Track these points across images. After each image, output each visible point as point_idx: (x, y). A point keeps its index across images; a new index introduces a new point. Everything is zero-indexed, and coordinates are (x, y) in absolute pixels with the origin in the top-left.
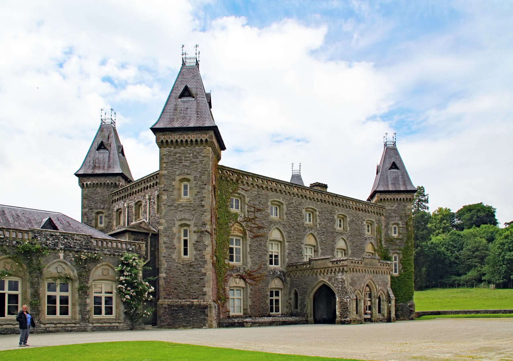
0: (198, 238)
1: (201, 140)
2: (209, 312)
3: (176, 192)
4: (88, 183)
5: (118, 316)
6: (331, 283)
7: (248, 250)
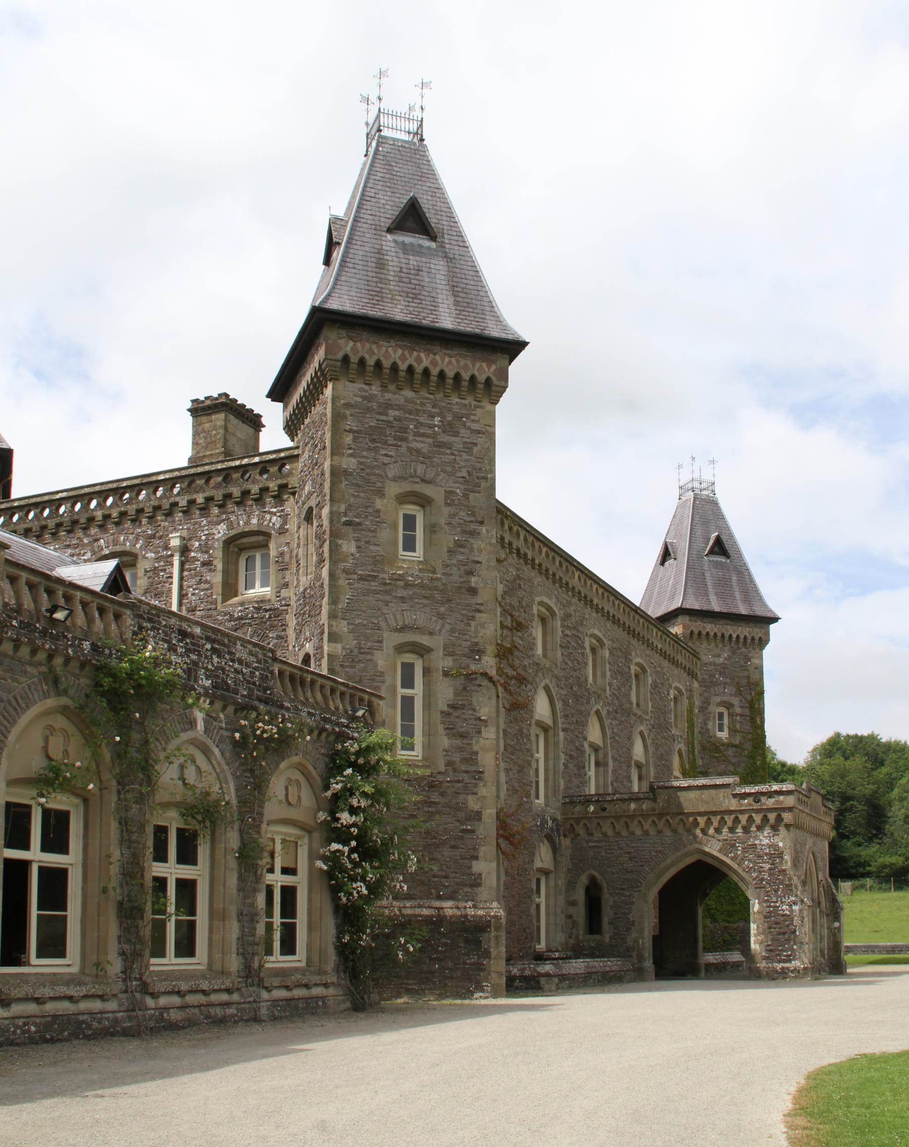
0: (456, 694)
1: (473, 379)
2: (493, 943)
3: (384, 535)
5: (316, 958)
6: (732, 859)
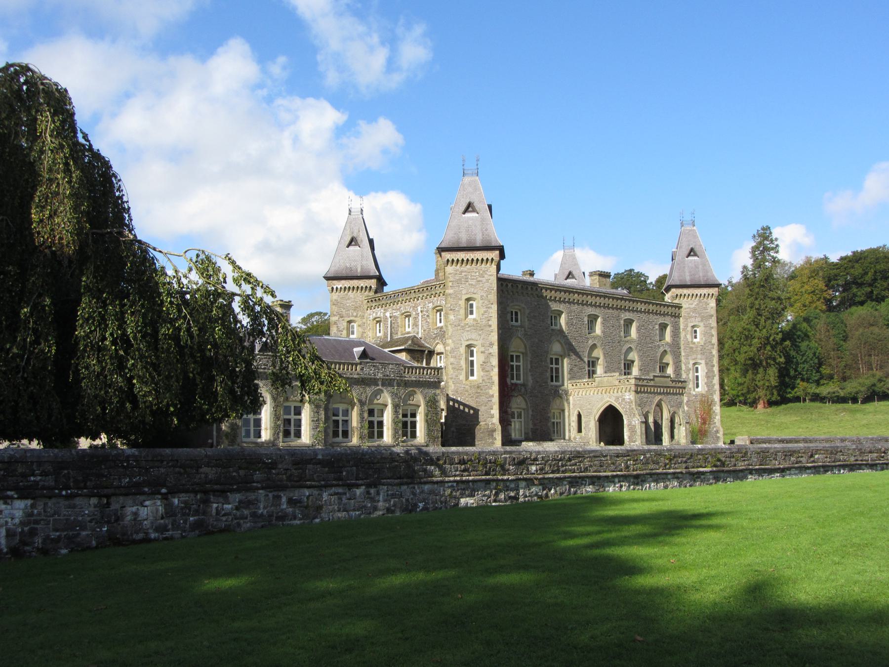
7: (529, 367)
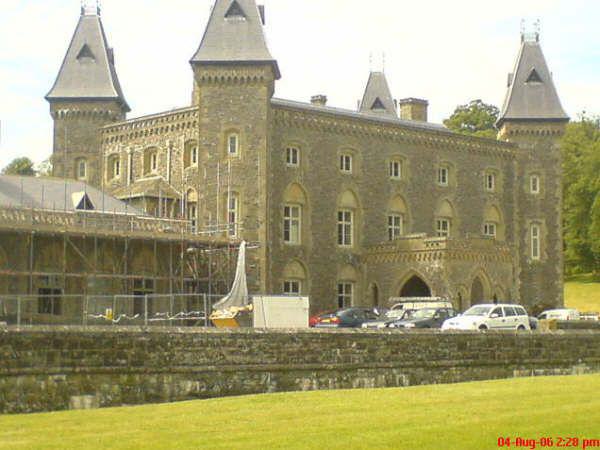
3: (220, 148)
4: (65, 111)
7: (310, 223)
